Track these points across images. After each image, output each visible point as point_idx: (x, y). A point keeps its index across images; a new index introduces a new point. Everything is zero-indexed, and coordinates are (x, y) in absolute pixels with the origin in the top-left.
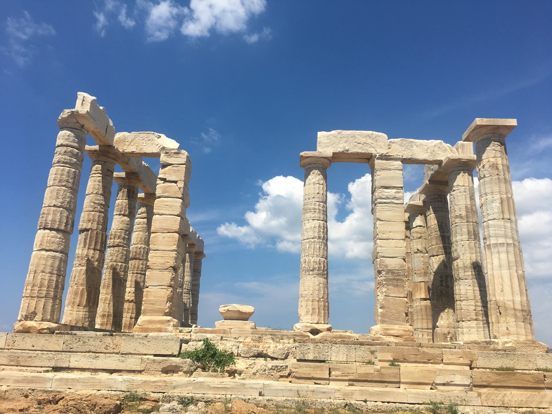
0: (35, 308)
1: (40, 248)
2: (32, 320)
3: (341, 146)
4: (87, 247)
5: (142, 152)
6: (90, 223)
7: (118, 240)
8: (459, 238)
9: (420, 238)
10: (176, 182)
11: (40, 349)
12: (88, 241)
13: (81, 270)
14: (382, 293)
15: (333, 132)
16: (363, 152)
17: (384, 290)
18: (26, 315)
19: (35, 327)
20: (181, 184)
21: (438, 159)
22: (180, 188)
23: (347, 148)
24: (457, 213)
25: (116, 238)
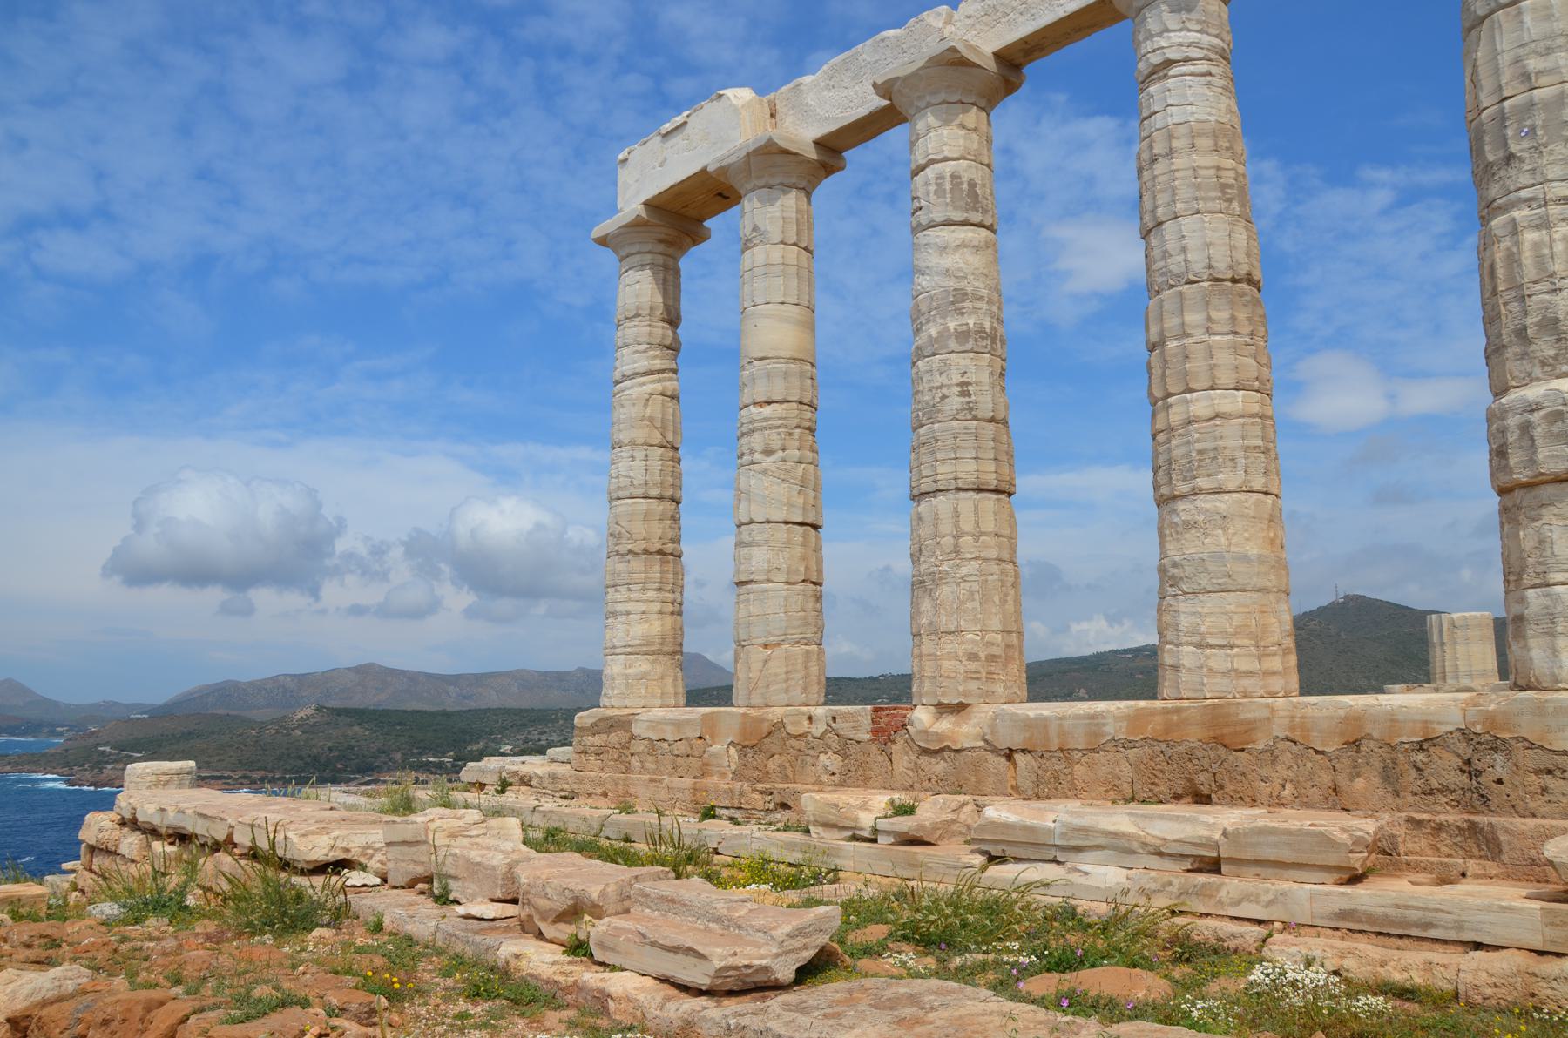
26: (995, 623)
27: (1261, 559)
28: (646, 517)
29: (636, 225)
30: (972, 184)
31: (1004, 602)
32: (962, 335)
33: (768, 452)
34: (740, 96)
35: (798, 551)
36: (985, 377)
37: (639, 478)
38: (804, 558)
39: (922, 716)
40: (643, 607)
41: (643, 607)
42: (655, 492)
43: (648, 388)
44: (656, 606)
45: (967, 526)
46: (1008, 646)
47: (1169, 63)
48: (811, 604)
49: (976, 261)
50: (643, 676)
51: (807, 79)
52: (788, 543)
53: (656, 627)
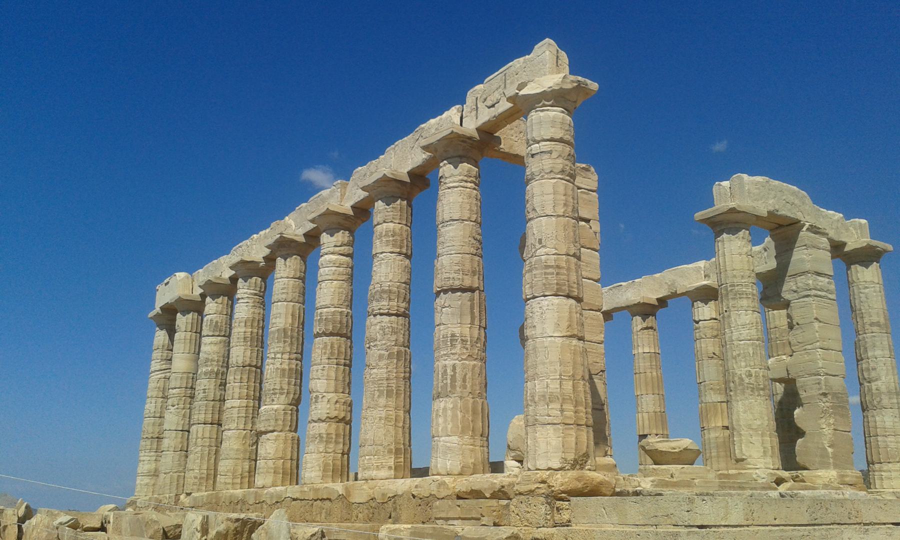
0: (587, 447)
1: (569, 334)
2: (582, 469)
3: (771, 202)
4: (477, 322)
5: (512, 152)
6: (477, 277)
7: (404, 305)
8: (878, 353)
9: (715, 337)
10: (587, 221)
11: (783, 523)
12: (476, 311)
13: (474, 366)
14: (829, 425)
15: (759, 179)
16: (792, 216)
17: (832, 421)
18: (575, 460)
19: (608, 483)
20: (596, 226)
21: (843, 240)
22: (595, 233)
23: (777, 207)
24: (875, 319)
25: (401, 300)
26: (205, 467)
27: (237, 450)
28: (154, 424)
29: (157, 315)
30: (217, 322)
31: (209, 460)
32: (206, 373)
33: (173, 406)
34: (181, 275)
35: (179, 440)
36: (212, 387)
37: (153, 410)
38: (181, 442)
39: (182, 497)
40: (148, 458)
41: (148, 458)
42: (158, 415)
43: (159, 376)
44: (154, 458)
45: (200, 435)
46: (208, 475)
47: (239, 299)
48: (183, 458)
49: (215, 348)
50: (147, 484)
51: (201, 270)
52: (176, 437)
53: (153, 466)
